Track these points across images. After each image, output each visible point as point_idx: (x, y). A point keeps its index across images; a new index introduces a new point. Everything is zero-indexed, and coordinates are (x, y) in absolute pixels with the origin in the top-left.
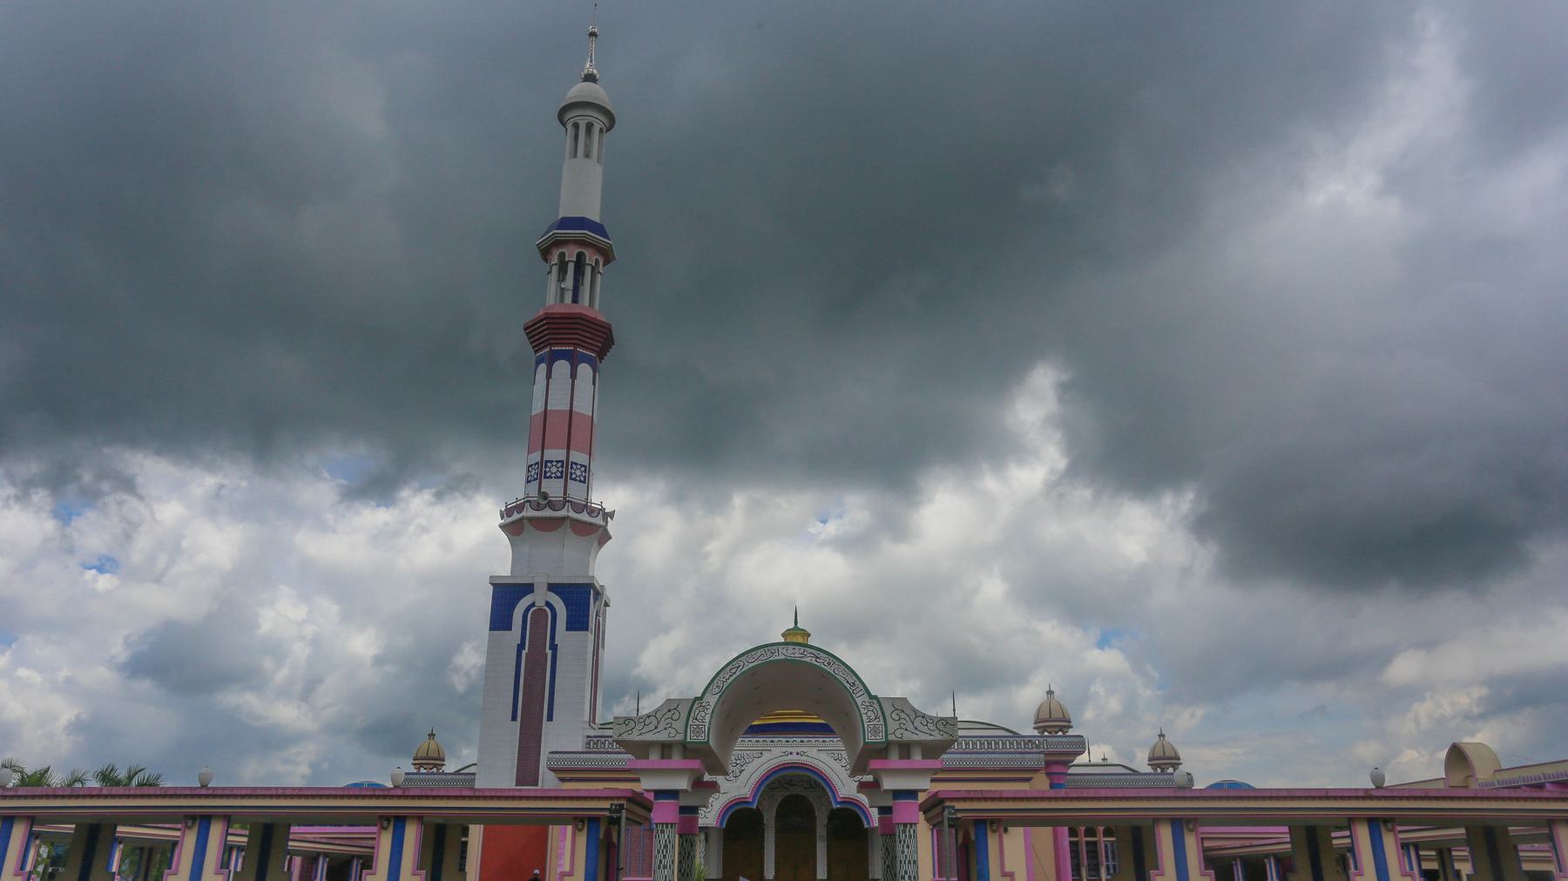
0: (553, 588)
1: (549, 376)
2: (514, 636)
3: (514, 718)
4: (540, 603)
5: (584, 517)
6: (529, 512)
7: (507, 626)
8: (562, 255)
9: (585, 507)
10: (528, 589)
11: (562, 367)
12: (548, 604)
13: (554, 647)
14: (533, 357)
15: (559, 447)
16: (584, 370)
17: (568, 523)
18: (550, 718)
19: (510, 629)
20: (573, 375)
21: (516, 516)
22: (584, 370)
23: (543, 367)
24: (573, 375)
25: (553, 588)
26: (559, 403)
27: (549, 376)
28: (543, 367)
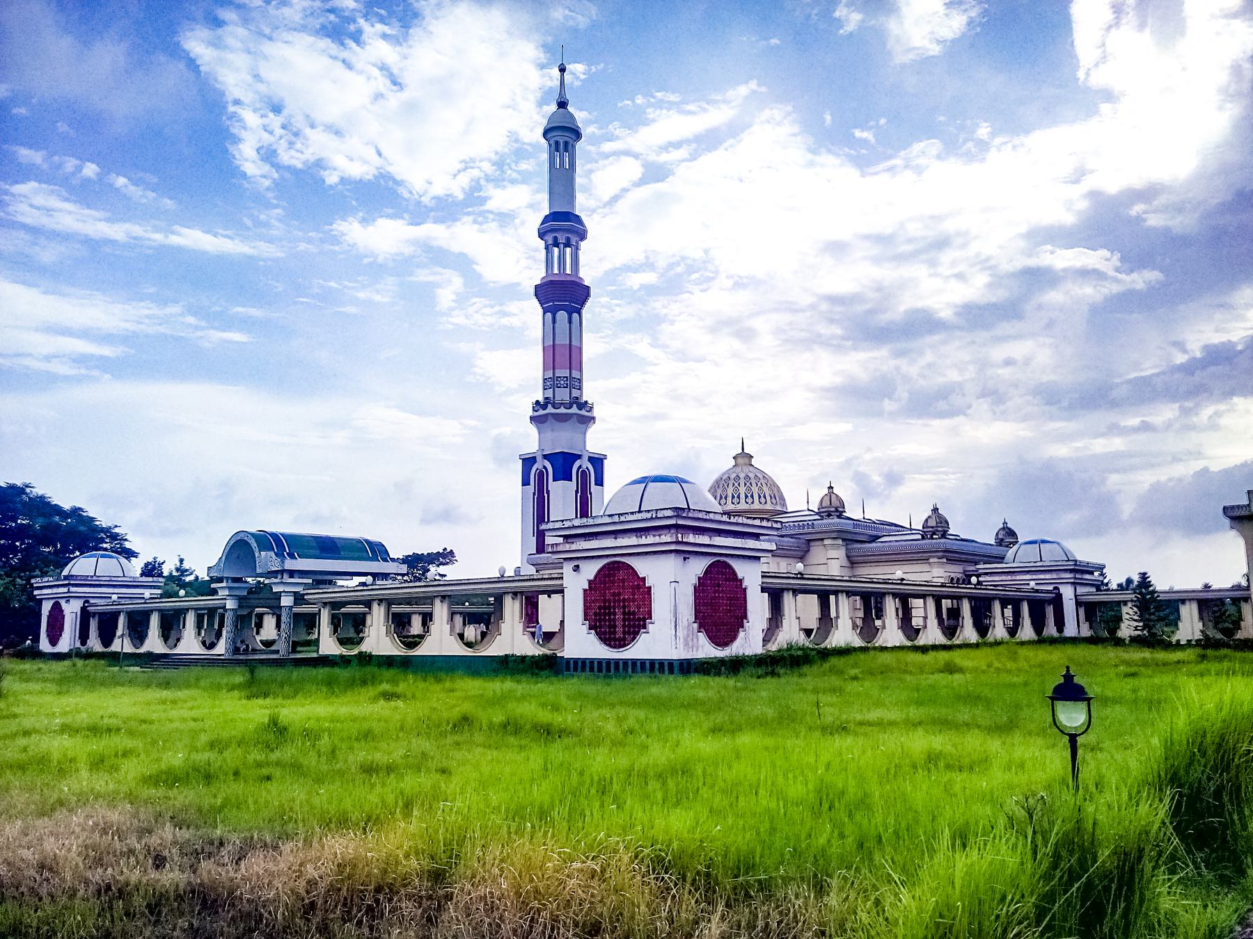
1: (554, 321)
5: (583, 412)
6: (550, 410)
8: (555, 238)
9: (583, 405)
11: (562, 315)
14: (540, 311)
16: (575, 315)
17: (575, 418)
20: (570, 322)
21: (541, 412)
22: (575, 315)
23: (549, 315)
24: (570, 322)
26: (562, 340)
27: (554, 321)
28: (549, 315)
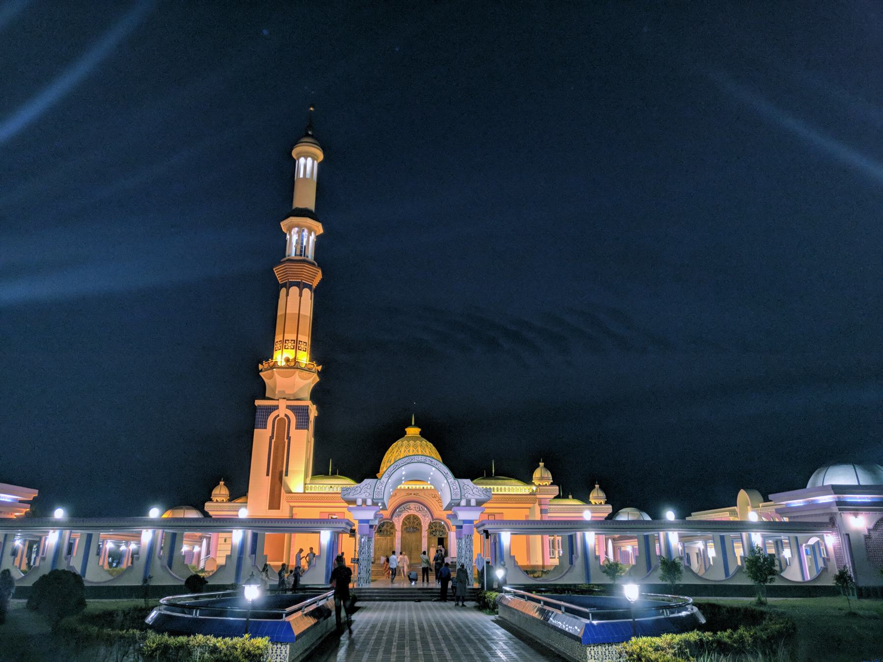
0: (288, 407)
1: (287, 295)
2: (268, 432)
3: (268, 475)
4: (282, 415)
7: (265, 428)
10: (277, 407)
11: (294, 290)
12: (286, 415)
13: (289, 438)
15: (292, 333)
18: (286, 475)
19: (265, 428)
20: (301, 295)
24: (301, 295)
25: (288, 407)
